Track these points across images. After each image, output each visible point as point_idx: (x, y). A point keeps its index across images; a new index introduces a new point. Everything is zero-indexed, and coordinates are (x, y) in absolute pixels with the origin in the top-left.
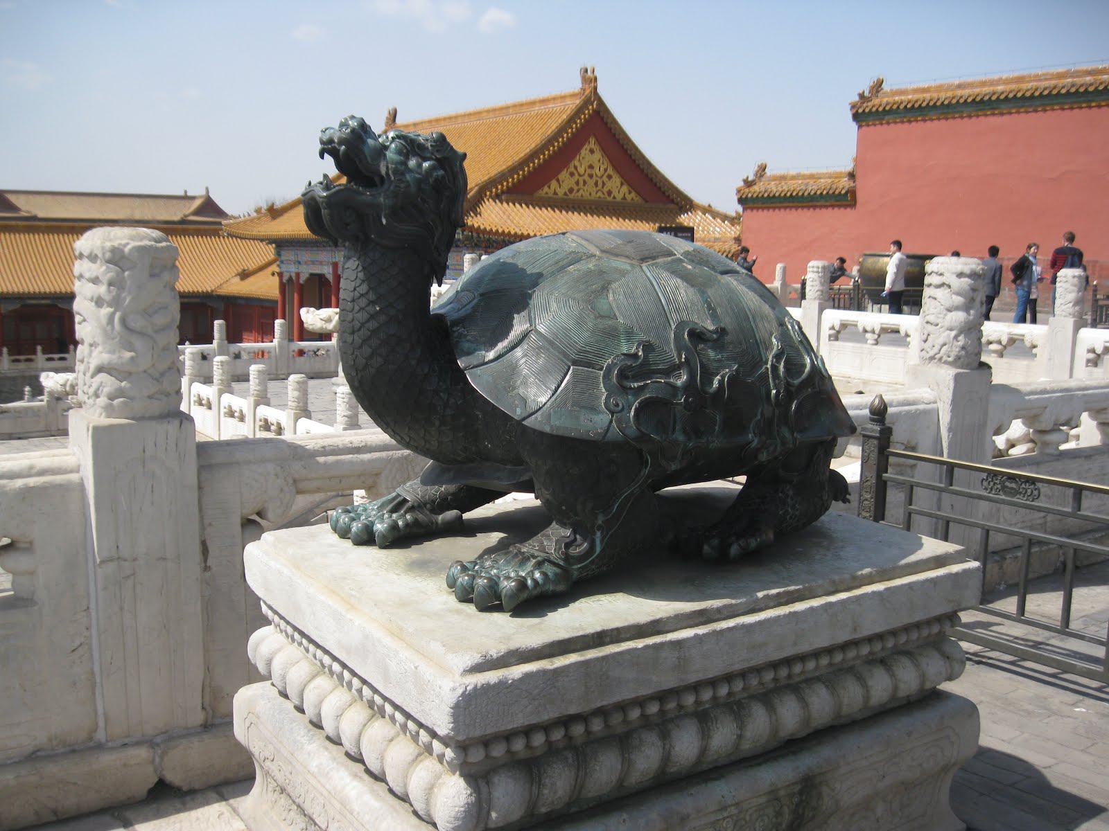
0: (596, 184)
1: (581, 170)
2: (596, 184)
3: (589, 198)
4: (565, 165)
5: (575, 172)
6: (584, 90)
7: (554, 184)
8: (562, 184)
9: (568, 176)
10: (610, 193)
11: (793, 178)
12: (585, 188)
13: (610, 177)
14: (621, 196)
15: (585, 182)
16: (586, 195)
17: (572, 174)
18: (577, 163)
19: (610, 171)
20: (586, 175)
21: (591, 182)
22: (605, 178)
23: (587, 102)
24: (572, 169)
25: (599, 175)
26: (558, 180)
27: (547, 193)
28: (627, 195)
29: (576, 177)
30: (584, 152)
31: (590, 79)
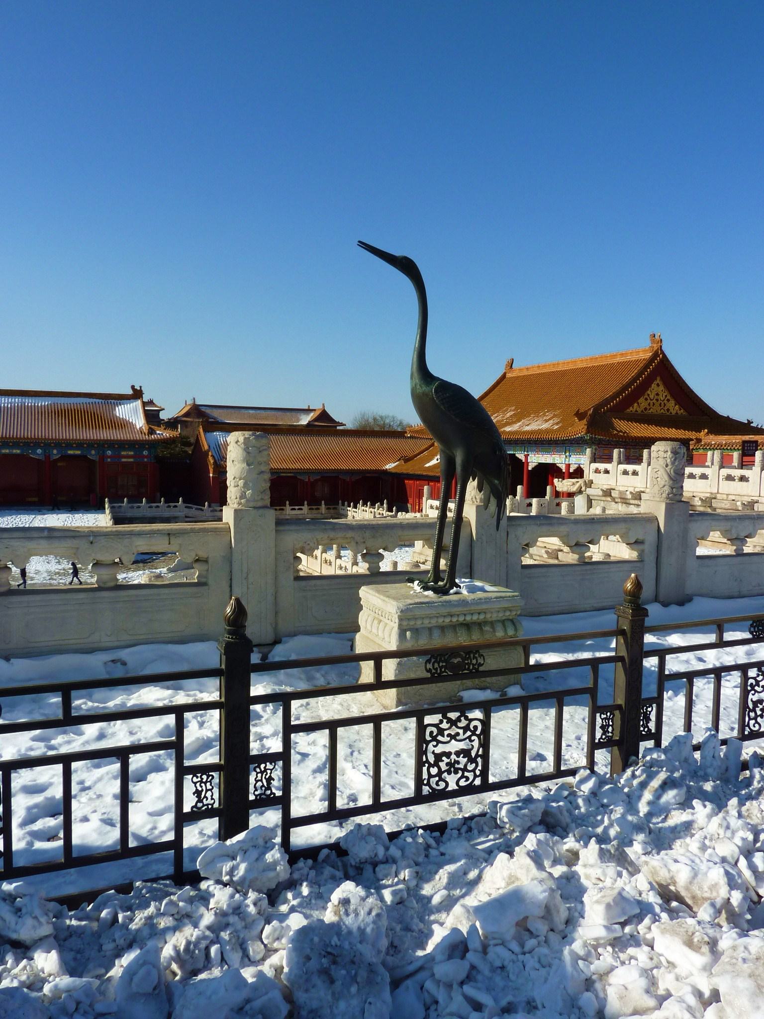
0: (660, 405)
1: (652, 397)
2: (660, 405)
10: (668, 410)
13: (668, 400)
16: (654, 411)
17: (646, 399)
19: (669, 397)
21: (657, 404)
23: (656, 355)
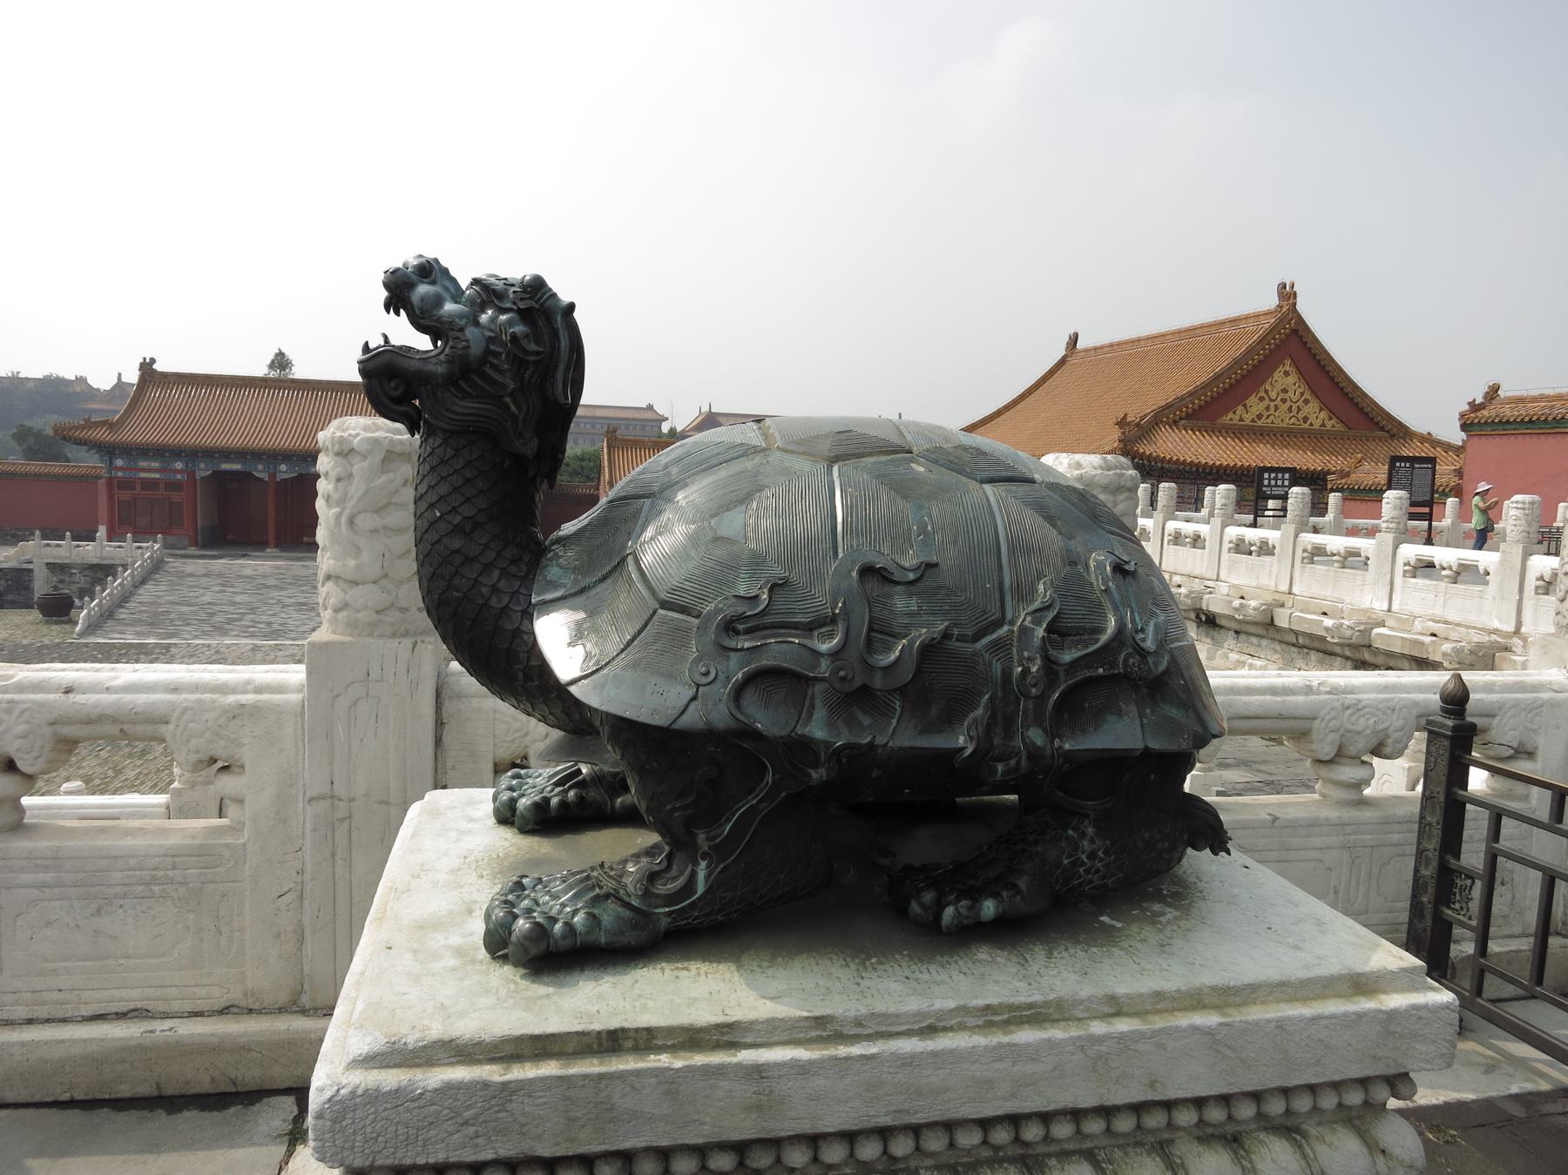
0: (1290, 409)
1: (1273, 395)
2: (1290, 409)
4: (1255, 388)
6: (1280, 306)
7: (1240, 409)
8: (1251, 410)
10: (1306, 419)
11: (1535, 399)
14: (1319, 422)
15: (1276, 408)
18: (1268, 387)
19: (1307, 395)
21: (1285, 407)
24: (1262, 394)
29: (1267, 402)
30: (1278, 375)
31: (1287, 294)
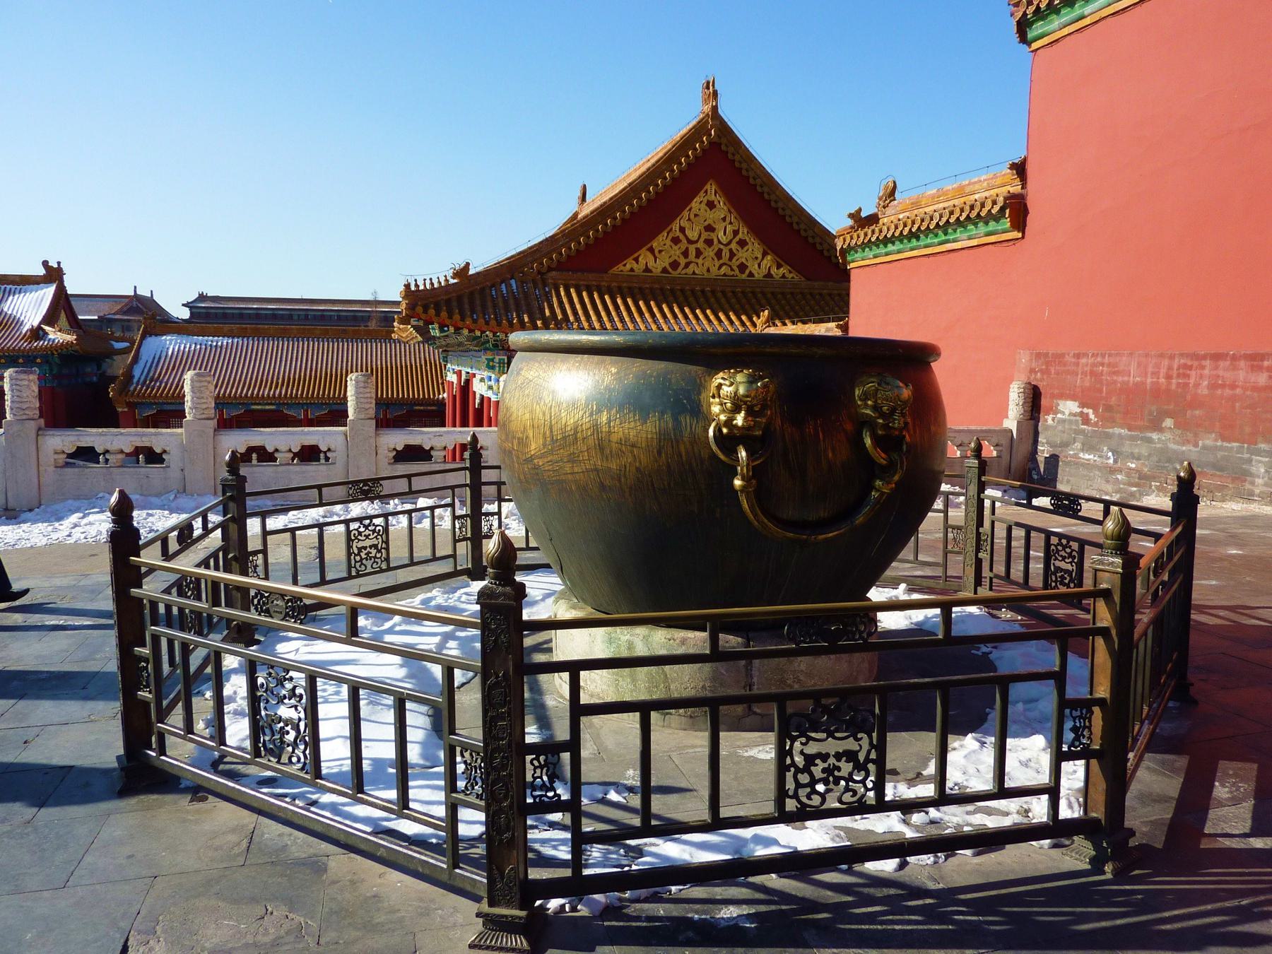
0: (719, 254)
2: (719, 254)
3: (706, 275)
5: (682, 237)
9: (668, 242)
10: (742, 267)
12: (700, 261)
15: (699, 253)
17: (676, 241)
18: (684, 223)
19: (744, 233)
20: (702, 240)
21: (710, 253)
22: (734, 246)
25: (724, 240)
26: (651, 250)
27: (632, 270)
28: (774, 271)
30: (697, 204)
